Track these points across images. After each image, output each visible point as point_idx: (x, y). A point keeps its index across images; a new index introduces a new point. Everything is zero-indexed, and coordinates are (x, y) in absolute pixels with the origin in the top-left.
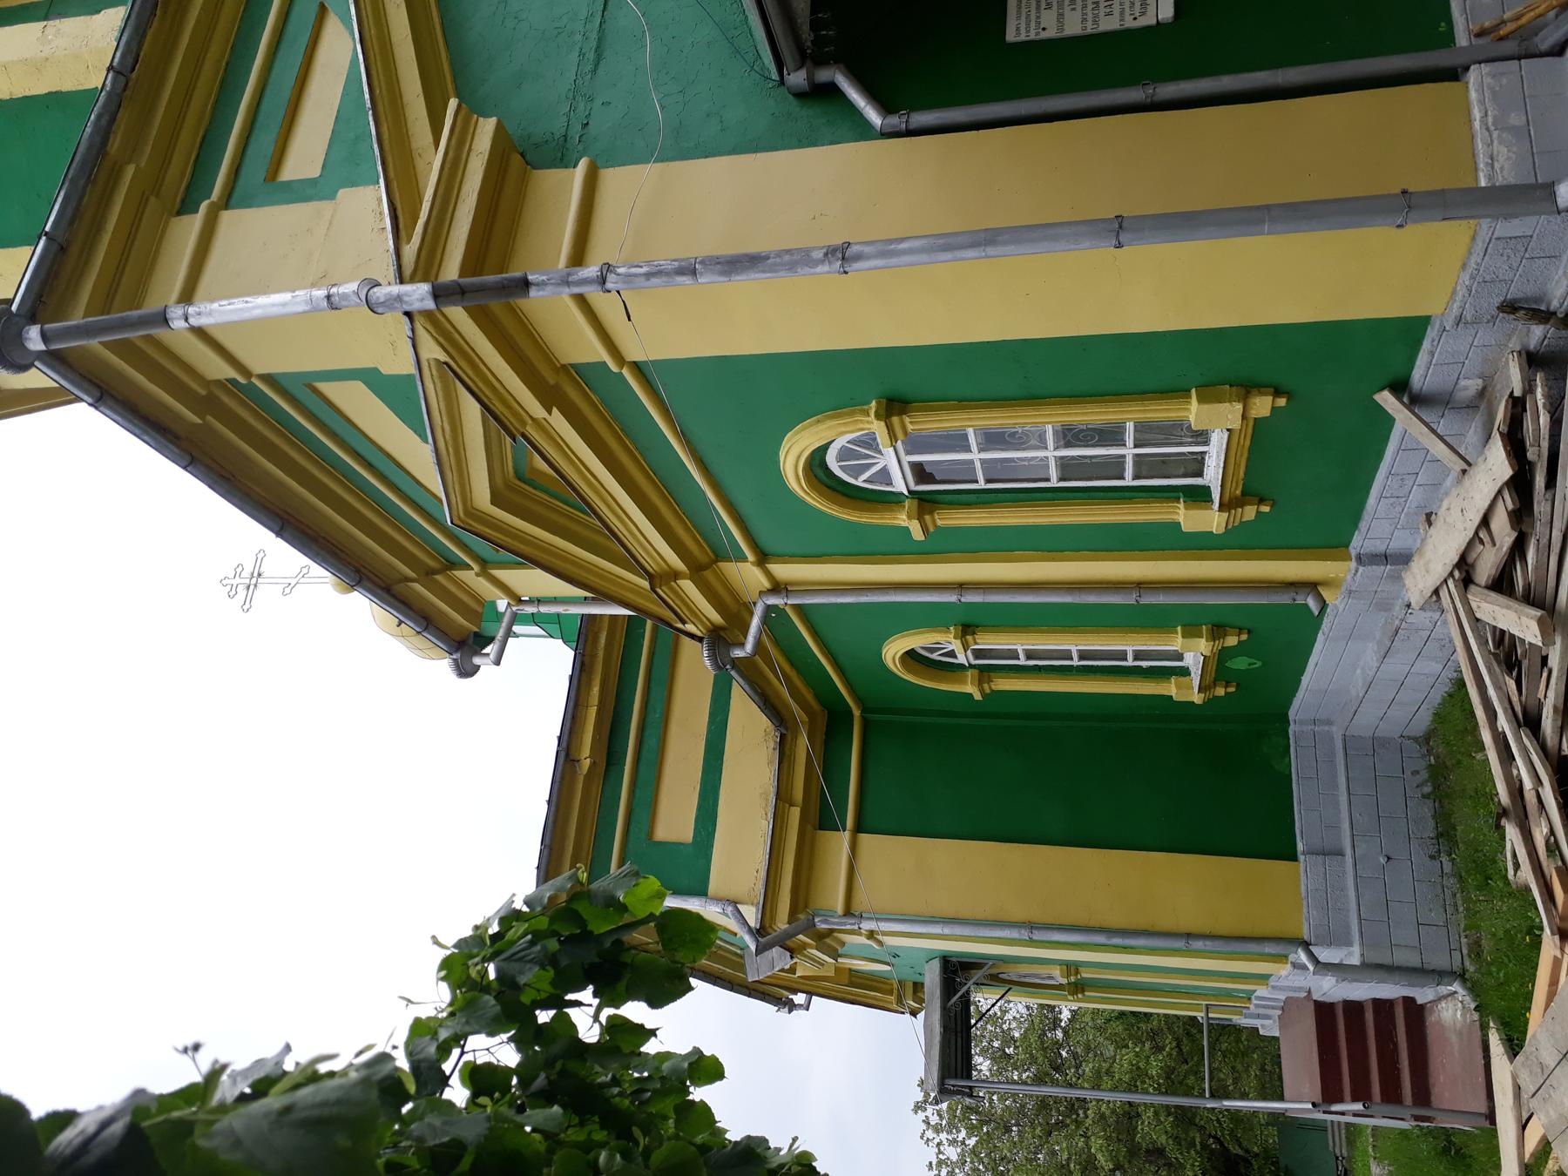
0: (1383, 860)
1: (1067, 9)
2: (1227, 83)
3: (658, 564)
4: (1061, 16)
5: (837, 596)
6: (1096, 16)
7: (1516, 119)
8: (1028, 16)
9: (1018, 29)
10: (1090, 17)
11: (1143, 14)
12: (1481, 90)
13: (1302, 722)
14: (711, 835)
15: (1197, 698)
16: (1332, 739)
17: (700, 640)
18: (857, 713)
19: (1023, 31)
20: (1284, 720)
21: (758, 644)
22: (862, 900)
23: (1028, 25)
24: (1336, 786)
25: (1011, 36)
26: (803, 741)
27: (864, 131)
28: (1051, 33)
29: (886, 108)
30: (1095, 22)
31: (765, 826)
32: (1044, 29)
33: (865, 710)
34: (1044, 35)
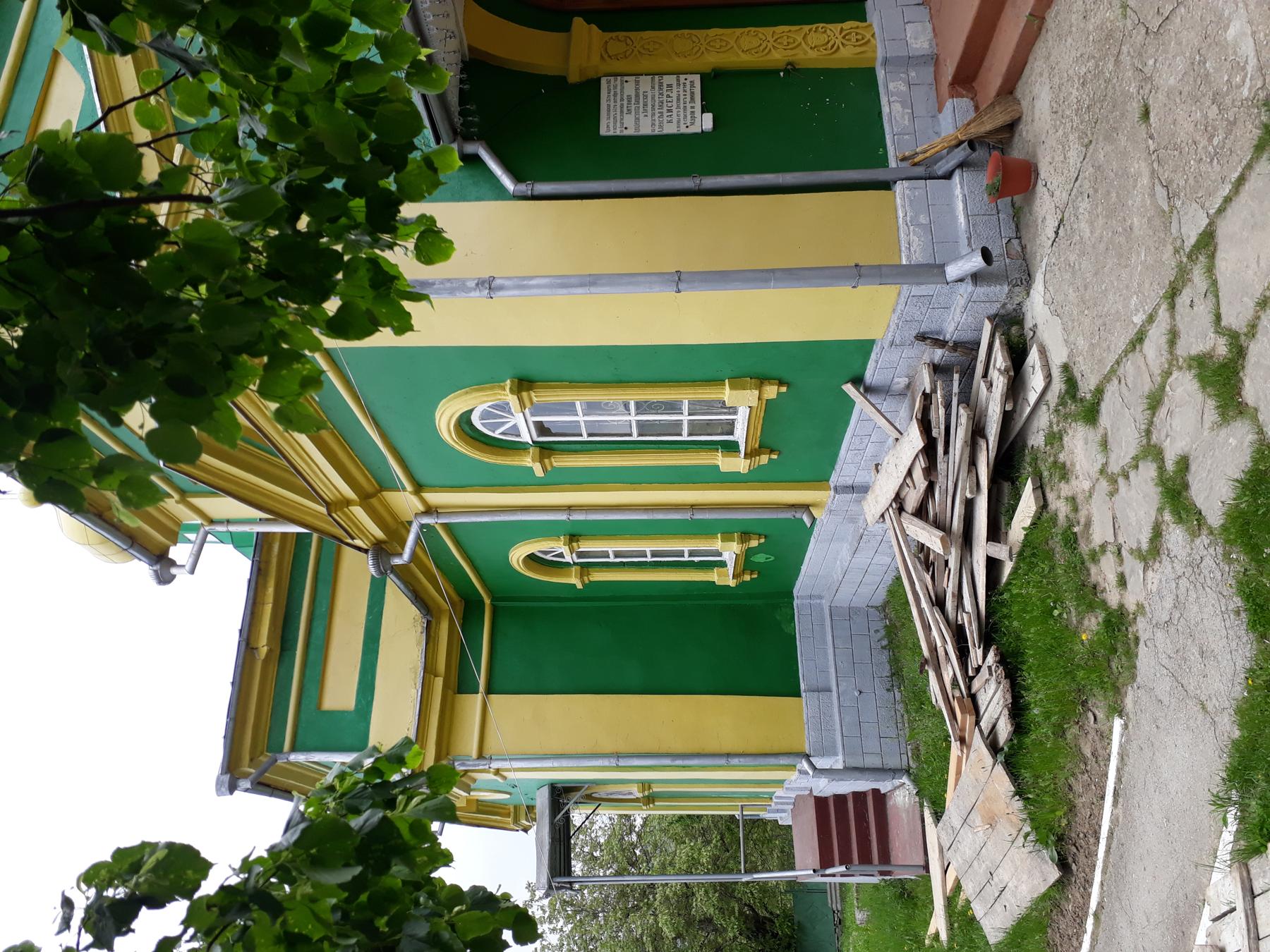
0: (856, 694)
1: (642, 116)
3: (334, 495)
4: (637, 119)
5: (477, 516)
7: (923, 219)
8: (615, 118)
9: (608, 126)
10: (657, 123)
11: (692, 124)
12: (903, 198)
13: (802, 598)
14: (370, 703)
15: (732, 583)
16: (822, 609)
17: (366, 551)
18: (487, 601)
19: (612, 128)
20: (790, 595)
21: (414, 555)
22: (492, 746)
23: (615, 122)
24: (825, 642)
25: (603, 131)
26: (444, 626)
27: (500, 193)
28: (631, 132)
29: (518, 178)
30: (661, 127)
31: (414, 694)
32: (626, 128)
33: (494, 599)
34: (626, 133)
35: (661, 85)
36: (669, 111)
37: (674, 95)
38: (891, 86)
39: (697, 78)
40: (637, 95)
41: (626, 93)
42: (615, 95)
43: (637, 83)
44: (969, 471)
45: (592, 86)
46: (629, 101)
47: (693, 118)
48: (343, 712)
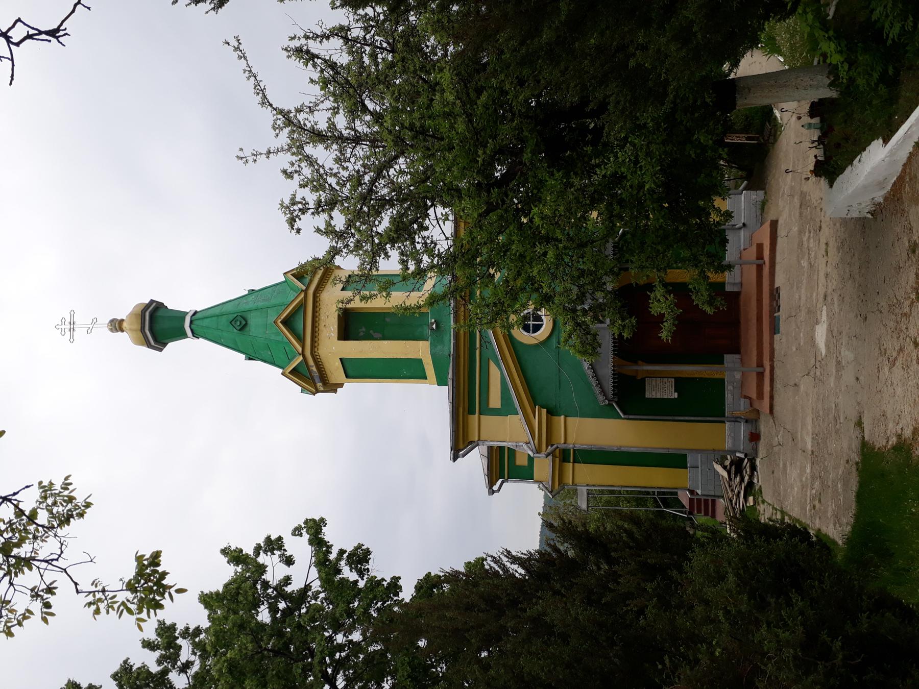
2: (687, 418)
25: (646, 397)
27: (620, 418)
29: (625, 414)
38: (729, 388)
39: (673, 380)
45: (643, 380)
48: (524, 466)
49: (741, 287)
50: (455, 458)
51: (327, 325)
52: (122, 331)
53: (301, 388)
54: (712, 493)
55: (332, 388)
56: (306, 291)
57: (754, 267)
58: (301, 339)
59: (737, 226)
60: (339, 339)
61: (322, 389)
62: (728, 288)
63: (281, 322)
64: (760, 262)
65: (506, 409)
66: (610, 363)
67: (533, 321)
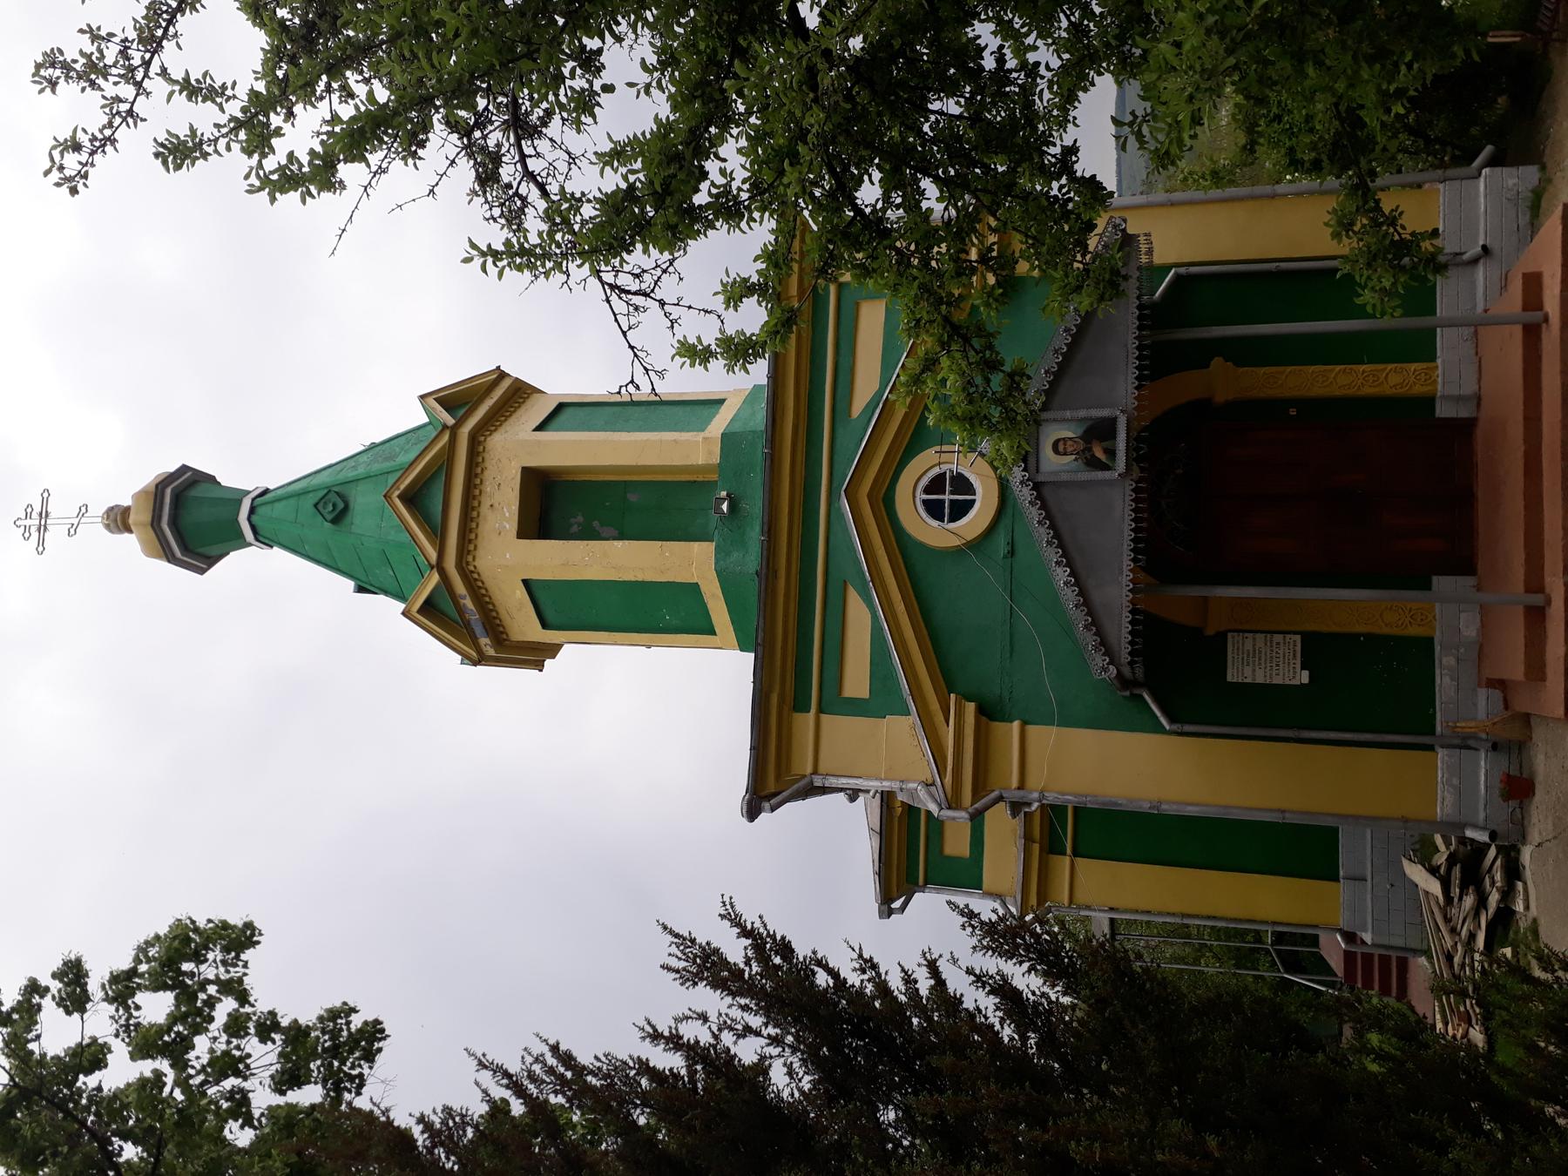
2: (1333, 735)
6: (1271, 674)
11: (1294, 677)
12: (1442, 763)
25: (1229, 679)
27: (1159, 729)
28: (1249, 680)
29: (1172, 720)
34: (1245, 681)
35: (1271, 642)
36: (1278, 665)
37: (1281, 652)
38: (1444, 660)
39: (1298, 638)
40: (1254, 651)
41: (1246, 649)
42: (1238, 649)
43: (1254, 639)
44: (1474, 919)
45: (1222, 637)
46: (1248, 655)
47: (1295, 673)
49: (1479, 405)
50: (752, 812)
51: (496, 505)
52: (130, 531)
53: (460, 657)
54: (1399, 942)
55: (534, 656)
56: (454, 430)
57: (1518, 331)
58: (438, 534)
59: (1465, 257)
60: (522, 534)
61: (491, 652)
62: (1443, 411)
63: (399, 497)
64: (1534, 316)
65: (880, 703)
66: (1126, 572)
67: (952, 493)
